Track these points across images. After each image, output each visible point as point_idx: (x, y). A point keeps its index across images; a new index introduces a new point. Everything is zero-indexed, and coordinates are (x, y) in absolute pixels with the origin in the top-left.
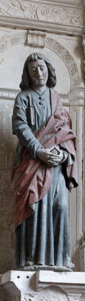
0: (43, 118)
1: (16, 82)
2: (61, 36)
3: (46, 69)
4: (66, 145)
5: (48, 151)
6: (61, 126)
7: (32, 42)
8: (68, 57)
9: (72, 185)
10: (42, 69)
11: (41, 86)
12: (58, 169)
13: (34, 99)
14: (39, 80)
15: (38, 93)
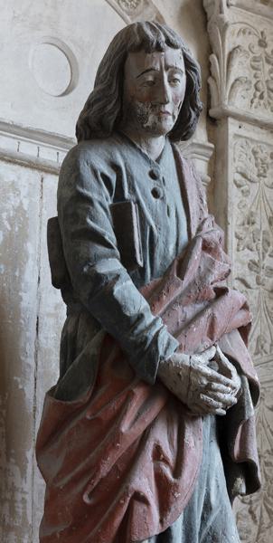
0: (166, 244)
9: (241, 484)
14: (160, 115)
15: (145, 157)
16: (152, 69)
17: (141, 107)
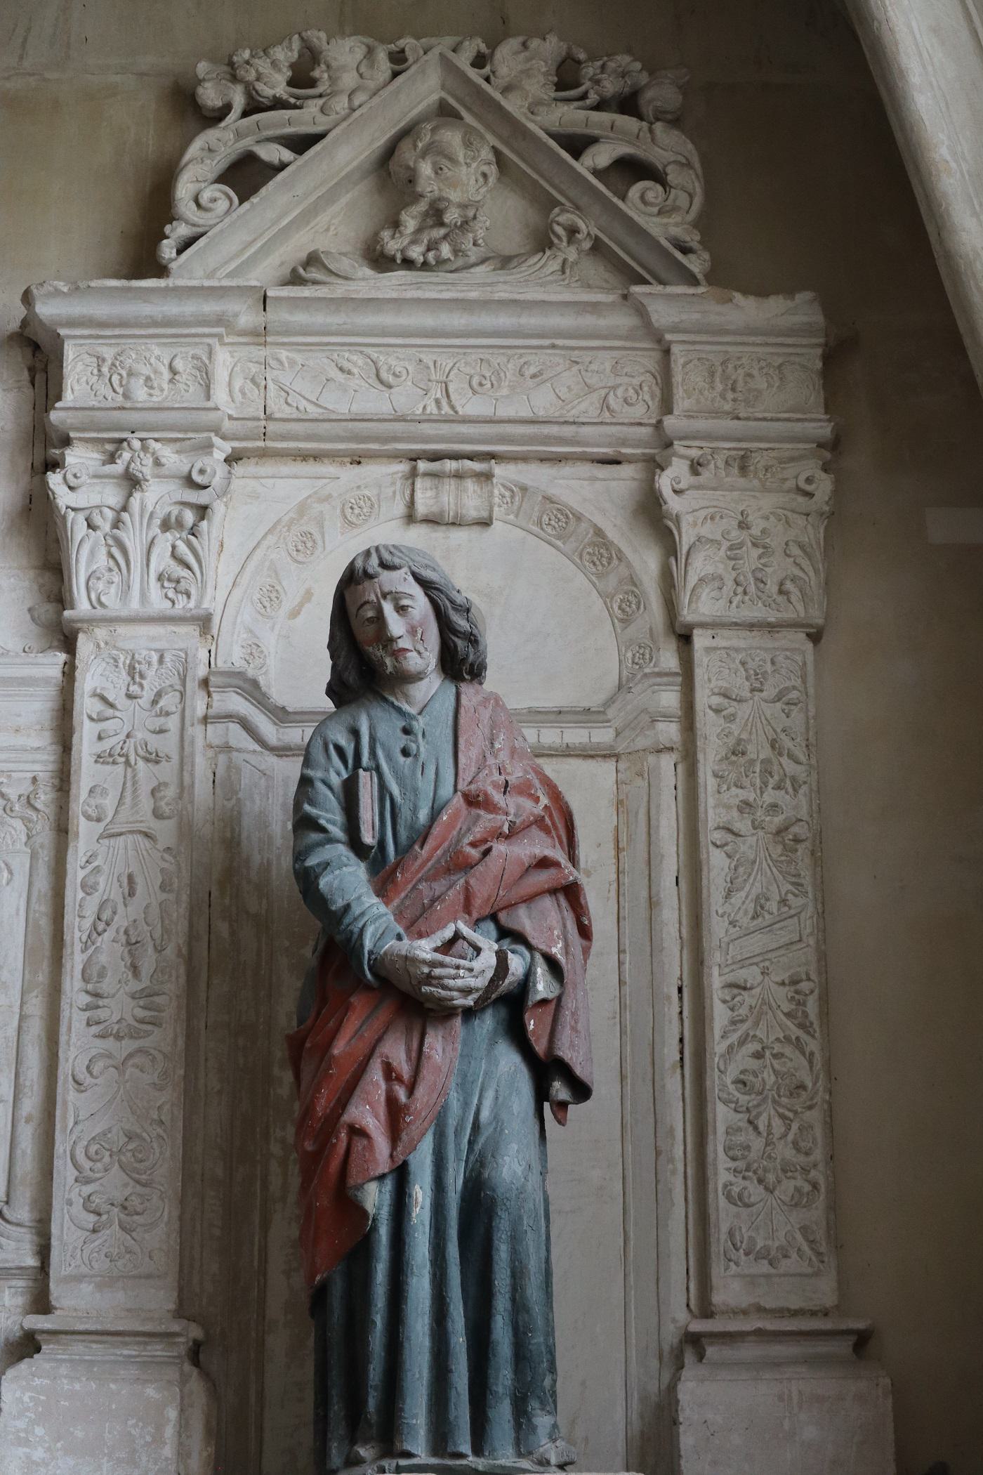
0: (415, 810)
1: (300, 666)
2: (567, 469)
3: (420, 604)
4: (524, 920)
5: (424, 949)
6: (500, 836)
7: (435, 509)
8: (600, 552)
9: (560, 1090)
10: (401, 609)
11: (405, 678)
12: (487, 1023)
13: (381, 734)
14: (398, 654)
15: (399, 711)
16: (367, 602)
17: (376, 652)
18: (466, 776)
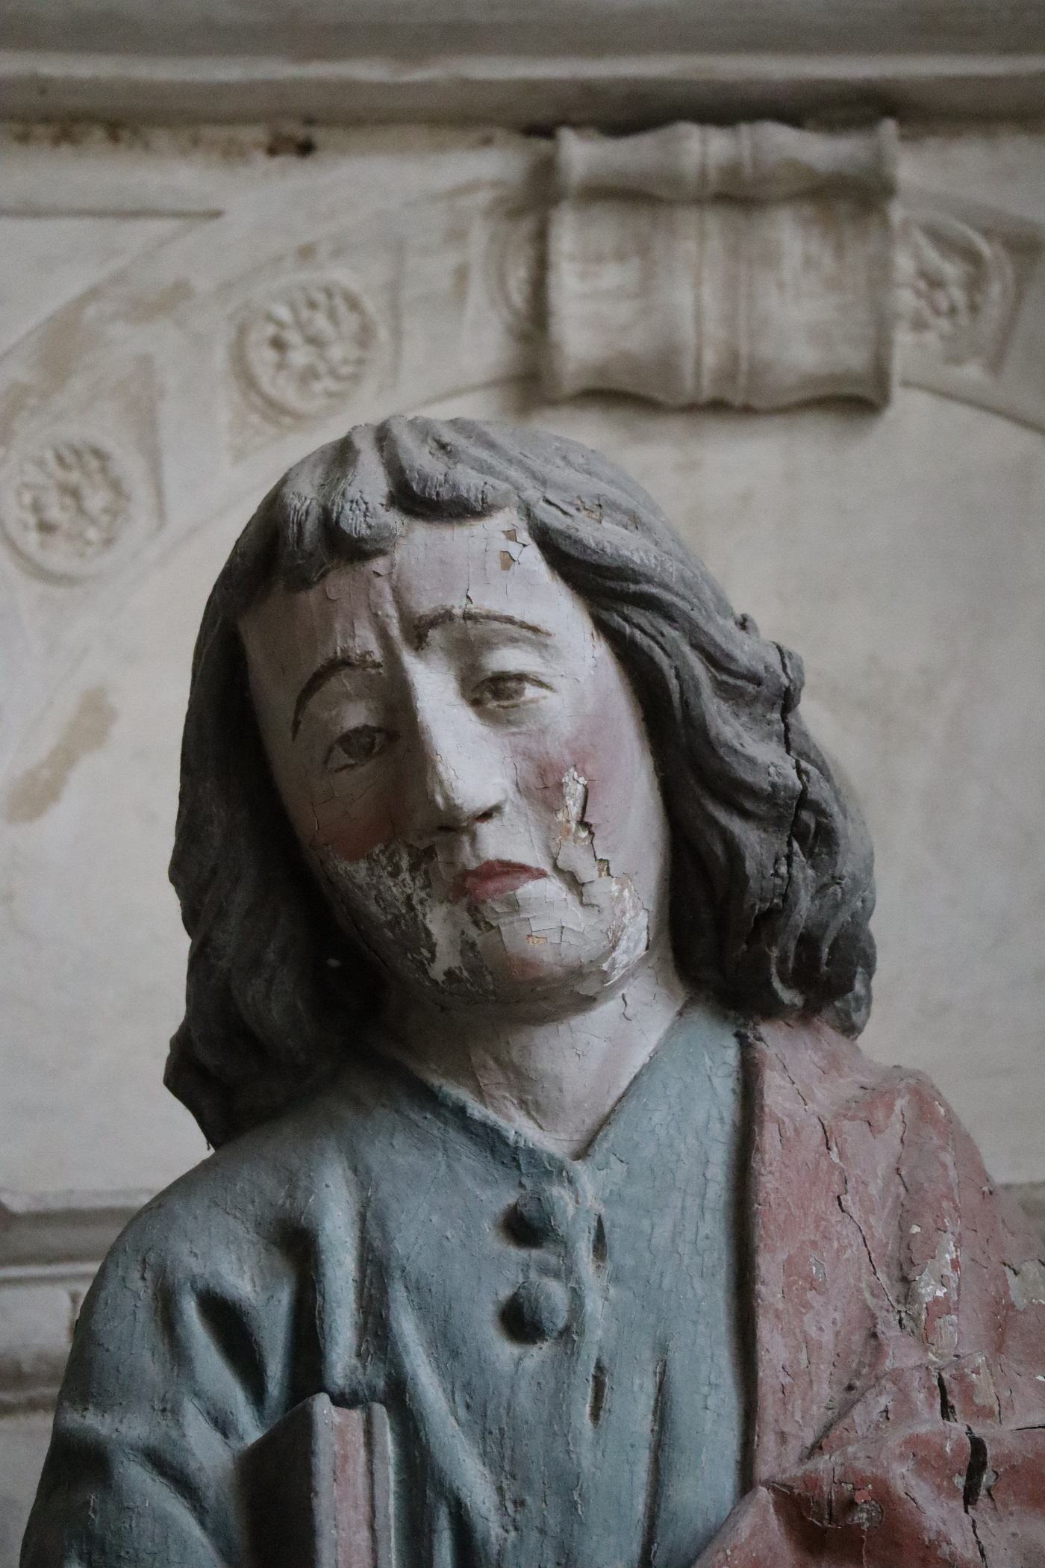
3: (574, 670)
7: (638, 342)
10: (491, 693)
13: (410, 1241)
15: (491, 1141)
17: (377, 883)
18: (792, 1421)
